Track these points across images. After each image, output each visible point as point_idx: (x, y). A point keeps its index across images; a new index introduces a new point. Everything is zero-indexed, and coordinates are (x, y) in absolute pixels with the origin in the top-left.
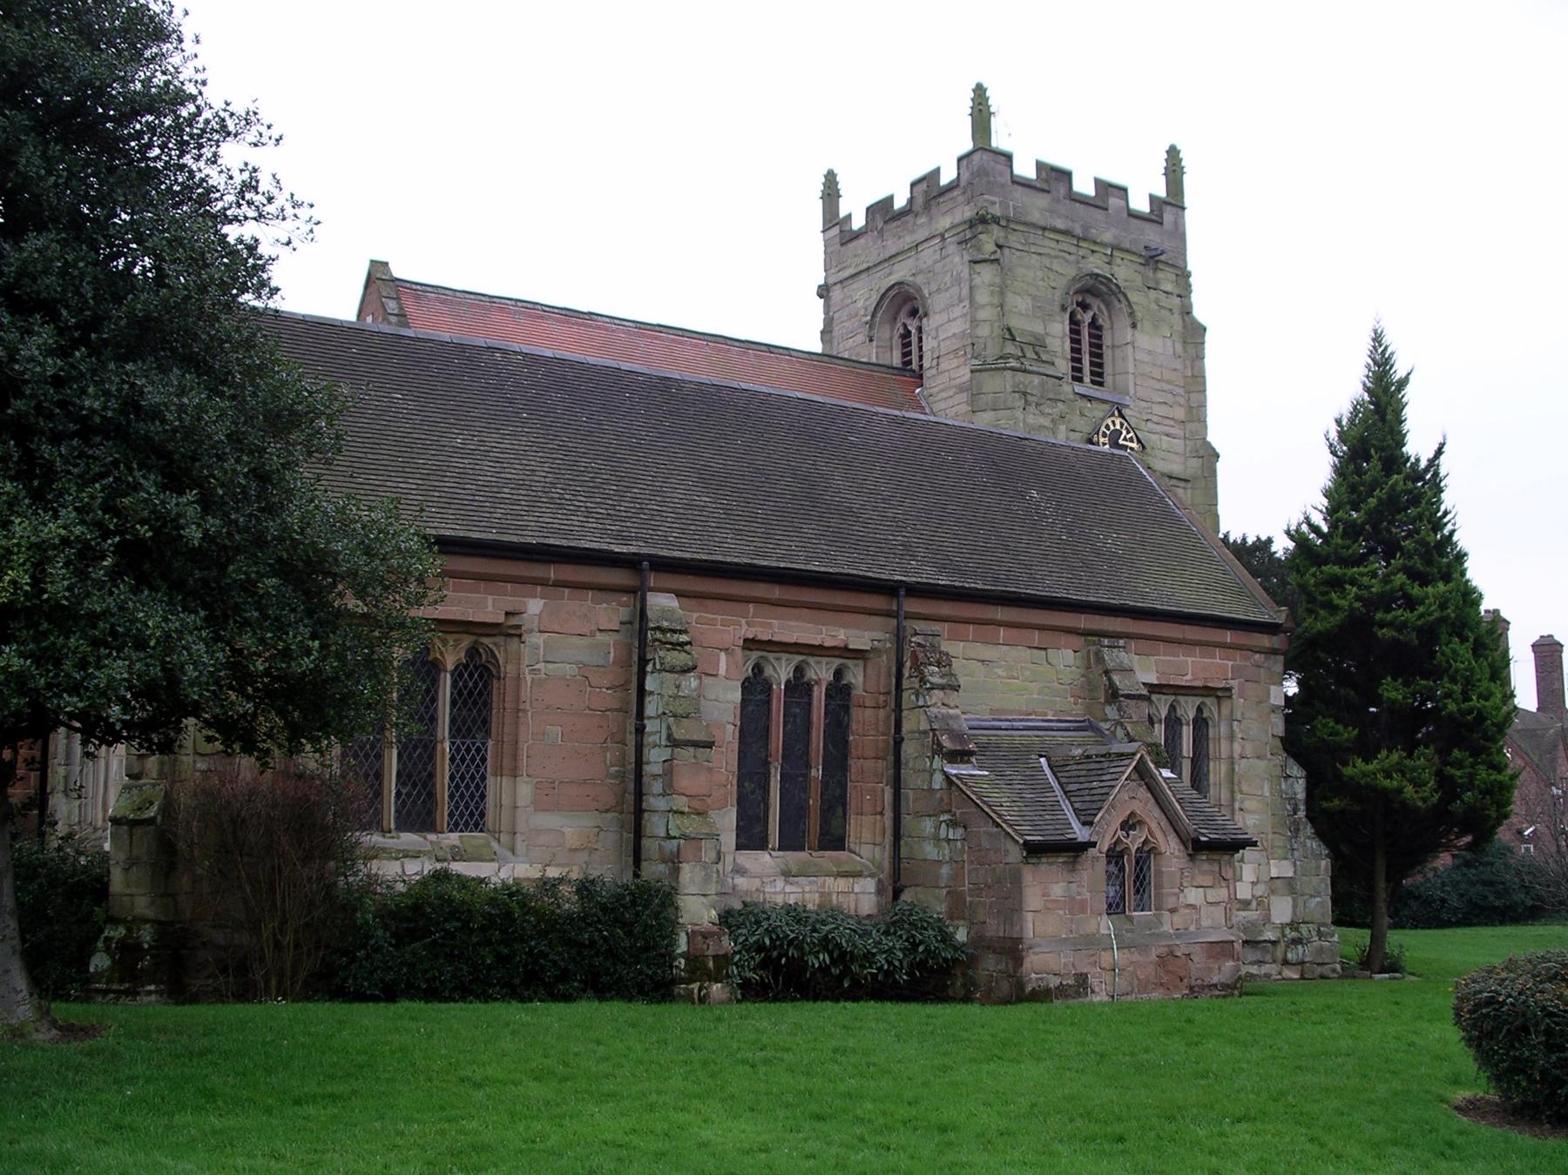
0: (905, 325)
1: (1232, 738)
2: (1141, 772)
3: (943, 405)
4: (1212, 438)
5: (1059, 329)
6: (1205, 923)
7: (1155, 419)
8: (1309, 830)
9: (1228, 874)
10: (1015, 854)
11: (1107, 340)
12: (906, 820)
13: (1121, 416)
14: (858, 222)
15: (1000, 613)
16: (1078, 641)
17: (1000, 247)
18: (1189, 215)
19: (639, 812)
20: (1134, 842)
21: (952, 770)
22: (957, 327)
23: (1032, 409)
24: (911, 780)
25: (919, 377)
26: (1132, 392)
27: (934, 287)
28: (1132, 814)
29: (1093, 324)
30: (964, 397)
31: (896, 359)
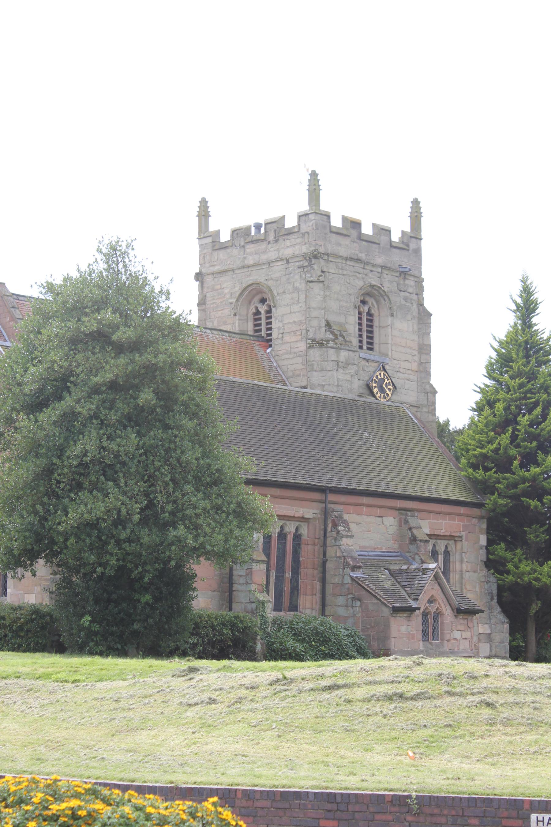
0: (257, 308)
1: (462, 561)
2: (436, 577)
3: (285, 362)
4: (434, 381)
5: (353, 319)
6: (462, 647)
7: (402, 370)
8: (499, 609)
9: (471, 625)
10: (386, 612)
11: (376, 323)
12: (328, 598)
13: (384, 370)
14: (225, 237)
15: (365, 500)
16: (397, 512)
17: (323, 272)
18: (424, 244)
19: (231, 591)
20: (432, 609)
21: (354, 575)
22: (297, 317)
23: (340, 370)
24: (332, 579)
25: (268, 342)
26: (390, 354)
27: (281, 291)
28: (432, 596)
29: (369, 314)
30: (300, 360)
31: (250, 328)
